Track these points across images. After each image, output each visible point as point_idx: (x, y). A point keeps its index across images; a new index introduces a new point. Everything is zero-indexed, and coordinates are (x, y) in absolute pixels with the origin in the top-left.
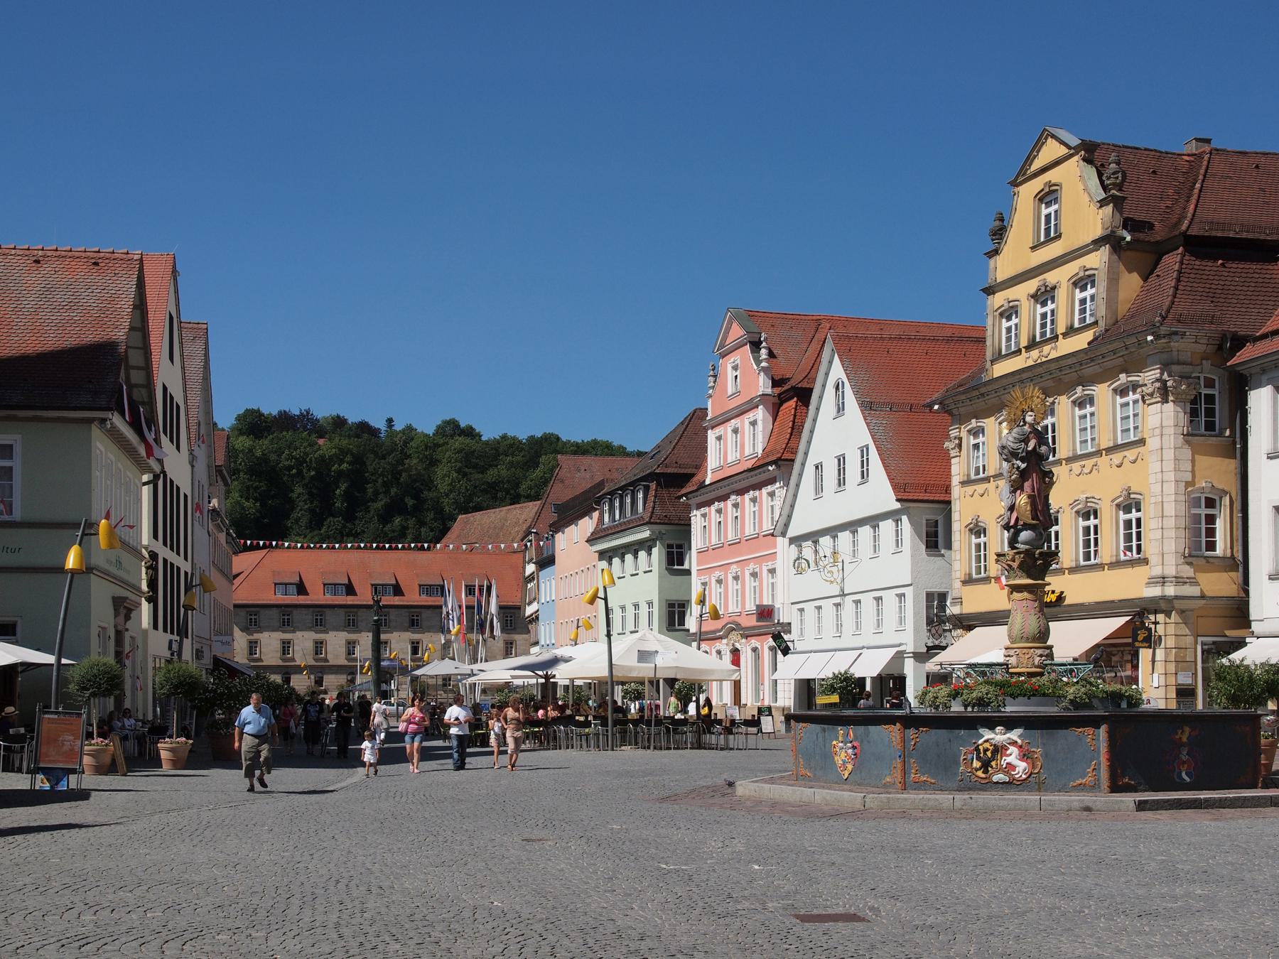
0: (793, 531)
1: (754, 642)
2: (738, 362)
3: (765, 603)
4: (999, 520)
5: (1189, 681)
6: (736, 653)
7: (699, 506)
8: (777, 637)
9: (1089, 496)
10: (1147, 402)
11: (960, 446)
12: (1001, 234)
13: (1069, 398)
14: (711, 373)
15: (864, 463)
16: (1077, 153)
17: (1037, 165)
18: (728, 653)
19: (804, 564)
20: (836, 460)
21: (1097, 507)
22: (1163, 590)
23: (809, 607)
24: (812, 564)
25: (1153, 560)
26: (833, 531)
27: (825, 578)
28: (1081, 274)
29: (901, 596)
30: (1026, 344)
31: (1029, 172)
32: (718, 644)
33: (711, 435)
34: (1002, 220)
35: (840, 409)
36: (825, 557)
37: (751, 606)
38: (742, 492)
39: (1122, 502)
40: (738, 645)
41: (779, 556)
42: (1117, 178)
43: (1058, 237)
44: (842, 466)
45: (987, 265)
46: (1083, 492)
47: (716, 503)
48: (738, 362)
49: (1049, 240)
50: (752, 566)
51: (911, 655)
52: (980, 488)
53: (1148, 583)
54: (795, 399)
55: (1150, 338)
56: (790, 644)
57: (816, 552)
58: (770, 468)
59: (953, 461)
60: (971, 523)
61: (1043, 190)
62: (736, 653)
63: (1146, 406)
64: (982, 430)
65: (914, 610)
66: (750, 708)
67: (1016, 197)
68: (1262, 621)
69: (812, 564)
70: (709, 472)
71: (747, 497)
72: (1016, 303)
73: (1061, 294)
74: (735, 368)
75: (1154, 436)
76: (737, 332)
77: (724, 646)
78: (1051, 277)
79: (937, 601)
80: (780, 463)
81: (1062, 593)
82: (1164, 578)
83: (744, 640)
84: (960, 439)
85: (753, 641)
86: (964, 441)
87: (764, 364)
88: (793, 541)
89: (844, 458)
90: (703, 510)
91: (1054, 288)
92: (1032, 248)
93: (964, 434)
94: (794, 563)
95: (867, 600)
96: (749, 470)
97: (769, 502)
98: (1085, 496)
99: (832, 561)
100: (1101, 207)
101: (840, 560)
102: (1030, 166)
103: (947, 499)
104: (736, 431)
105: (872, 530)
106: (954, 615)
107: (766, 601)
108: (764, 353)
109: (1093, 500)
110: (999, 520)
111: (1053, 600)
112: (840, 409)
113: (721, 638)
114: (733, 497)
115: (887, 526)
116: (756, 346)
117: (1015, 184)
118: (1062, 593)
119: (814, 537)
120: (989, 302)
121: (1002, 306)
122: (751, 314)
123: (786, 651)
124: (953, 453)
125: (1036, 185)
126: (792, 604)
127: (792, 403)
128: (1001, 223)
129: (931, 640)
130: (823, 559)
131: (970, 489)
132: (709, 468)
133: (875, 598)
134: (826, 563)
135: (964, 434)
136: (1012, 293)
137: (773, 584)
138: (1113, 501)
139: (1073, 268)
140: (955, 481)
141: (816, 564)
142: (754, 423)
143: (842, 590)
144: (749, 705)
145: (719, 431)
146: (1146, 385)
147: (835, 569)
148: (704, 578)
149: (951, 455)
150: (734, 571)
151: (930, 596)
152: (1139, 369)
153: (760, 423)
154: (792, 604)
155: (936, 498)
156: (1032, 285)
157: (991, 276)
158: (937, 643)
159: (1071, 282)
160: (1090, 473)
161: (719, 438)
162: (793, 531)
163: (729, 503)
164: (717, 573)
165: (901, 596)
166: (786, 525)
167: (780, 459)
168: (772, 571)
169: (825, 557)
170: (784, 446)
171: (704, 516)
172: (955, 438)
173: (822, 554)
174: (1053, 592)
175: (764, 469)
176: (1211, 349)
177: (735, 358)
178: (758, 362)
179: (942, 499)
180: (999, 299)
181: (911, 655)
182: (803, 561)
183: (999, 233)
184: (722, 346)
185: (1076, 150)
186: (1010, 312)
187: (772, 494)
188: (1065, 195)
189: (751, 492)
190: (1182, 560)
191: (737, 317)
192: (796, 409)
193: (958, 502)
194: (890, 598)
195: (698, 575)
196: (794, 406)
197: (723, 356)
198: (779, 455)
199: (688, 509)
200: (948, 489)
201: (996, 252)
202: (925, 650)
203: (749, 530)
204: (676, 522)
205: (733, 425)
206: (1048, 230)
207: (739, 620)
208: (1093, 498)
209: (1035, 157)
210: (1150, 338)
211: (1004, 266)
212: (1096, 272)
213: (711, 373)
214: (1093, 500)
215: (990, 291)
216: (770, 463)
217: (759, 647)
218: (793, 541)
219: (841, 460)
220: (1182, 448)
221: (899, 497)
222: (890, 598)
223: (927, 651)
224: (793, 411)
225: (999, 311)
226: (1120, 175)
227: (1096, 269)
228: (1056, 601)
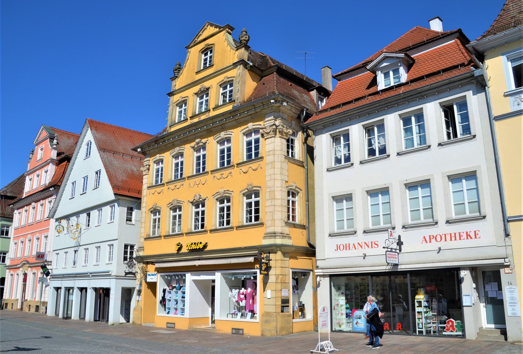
0: (57, 216)
1: (34, 270)
2: (44, 147)
3: (41, 251)
4: (168, 206)
5: (287, 295)
6: (25, 275)
7: (18, 209)
8: (44, 267)
9: (226, 190)
10: (266, 137)
11: (149, 169)
12: (179, 71)
13: (215, 140)
14: (32, 153)
15: (98, 181)
16: (224, 30)
17: (201, 38)
18: (22, 275)
19: (61, 229)
20: (83, 179)
21: (230, 195)
22: (275, 241)
23: (61, 252)
24: (66, 229)
25: (268, 223)
26: (77, 214)
27: (71, 236)
28: (225, 80)
29: (111, 246)
30: (191, 116)
31: (196, 41)
32: (18, 271)
33: (27, 178)
34: (180, 65)
35: (88, 154)
36: (72, 226)
37: (34, 253)
38: (37, 201)
39: (246, 192)
40: (26, 272)
41: (50, 230)
42: (246, 37)
43: (211, 66)
44: (89, 151)
45: (171, 84)
46: (222, 188)
47: (26, 207)
48: (44, 147)
49: (205, 68)
50: (37, 235)
51: (114, 277)
52: (159, 189)
53: (264, 237)
54: (66, 161)
55: (272, 101)
56: (50, 271)
57: (68, 223)
58: (51, 189)
59: (144, 177)
60: (152, 208)
61: (204, 48)
62: (25, 275)
63: (264, 139)
64: (162, 161)
65: (118, 251)
66: (28, 301)
67: (189, 53)
68: (325, 260)
69: (66, 229)
70: (24, 194)
71: (39, 204)
72: (186, 98)
73: (212, 92)
74: (42, 150)
75: (269, 155)
76: (44, 134)
77: (20, 272)
78: (207, 84)
79: (128, 248)
80: (56, 187)
81: (206, 243)
82: (275, 234)
83: (30, 269)
84: (149, 165)
85: (34, 270)
86: (151, 168)
87: (55, 146)
88: (57, 220)
89: (87, 178)
90: (20, 211)
91: (208, 89)
92: (196, 73)
93: (151, 163)
94: (56, 227)
95: (92, 249)
96: (42, 191)
97: (47, 204)
98: (224, 190)
99: (75, 228)
100: (237, 50)
101: (80, 228)
102: (199, 37)
103: (138, 197)
104: (38, 176)
105: (98, 212)
106: (140, 256)
107: (42, 251)
108: (55, 141)
109: (228, 192)
110: (168, 206)
111: (201, 248)
112: (88, 154)
113: (19, 268)
114: (33, 204)
115: (107, 210)
116: (52, 139)
117: (188, 47)
118: (206, 243)
119: (67, 217)
120: (171, 100)
121: (179, 100)
122: (53, 129)
123: (48, 274)
124: (144, 173)
125: (202, 46)
126: (54, 251)
127: (65, 163)
128: (179, 66)
129: (128, 269)
130: (71, 227)
131: (152, 190)
132: (25, 192)
133: (96, 247)
134: (73, 228)
135: (151, 163)
136: (184, 94)
137: (46, 243)
138: (241, 192)
139: (221, 78)
140: (145, 187)
141: (68, 228)
142: (46, 172)
143: (79, 244)
144: (28, 300)
145: (31, 176)
146: (266, 128)
147: (77, 233)
148: (16, 241)
149: (144, 174)
150: (29, 237)
151: (126, 246)
152: (261, 117)
153: (49, 173)
154: (54, 251)
155: (133, 196)
156: (196, 89)
157: (172, 89)
158: (130, 270)
159: (219, 85)
160: (226, 178)
161: (30, 180)
162: (57, 216)
163: (31, 207)
164: (22, 239)
165: (111, 246)
166: (55, 212)
167: (56, 185)
168: (46, 237)
169: (72, 226)
170: (58, 180)
171: (19, 213)
172: (147, 165)
173: (71, 224)
174: (201, 243)
175: (48, 190)
176: (296, 116)
177: (42, 145)
178: (52, 145)
179: (136, 196)
180: (176, 98)
181: (114, 277)
182: (61, 227)
183: (179, 69)
184: (37, 140)
185: (224, 28)
186: (184, 102)
187: (50, 202)
188: (216, 49)
189: (41, 201)
190: (284, 224)
191: (45, 128)
192: (66, 165)
193: (145, 198)
194: (105, 247)
195: (14, 240)
196: (65, 164)
197: (37, 145)
198: (56, 183)
199: (13, 210)
200: (140, 192)
201: (175, 77)
202: (124, 274)
203: (38, 218)
204: (7, 216)
205: (37, 173)
206: (205, 64)
207: (28, 260)
208: (228, 191)
209: (200, 35)
210: (272, 101)
211: (178, 84)
212: (234, 79)
213: (32, 153)
214: (228, 192)
215: (171, 94)
216: (51, 187)
217: (36, 272)
218: (57, 220)
219: (86, 178)
220: (283, 162)
221: (116, 193)
222: (105, 247)
223: (125, 275)
224: (65, 166)
225: (176, 103)
226: (247, 36)
227: (234, 77)
228: (203, 248)
